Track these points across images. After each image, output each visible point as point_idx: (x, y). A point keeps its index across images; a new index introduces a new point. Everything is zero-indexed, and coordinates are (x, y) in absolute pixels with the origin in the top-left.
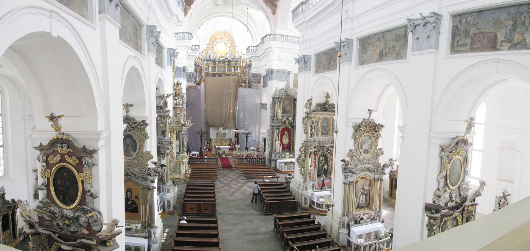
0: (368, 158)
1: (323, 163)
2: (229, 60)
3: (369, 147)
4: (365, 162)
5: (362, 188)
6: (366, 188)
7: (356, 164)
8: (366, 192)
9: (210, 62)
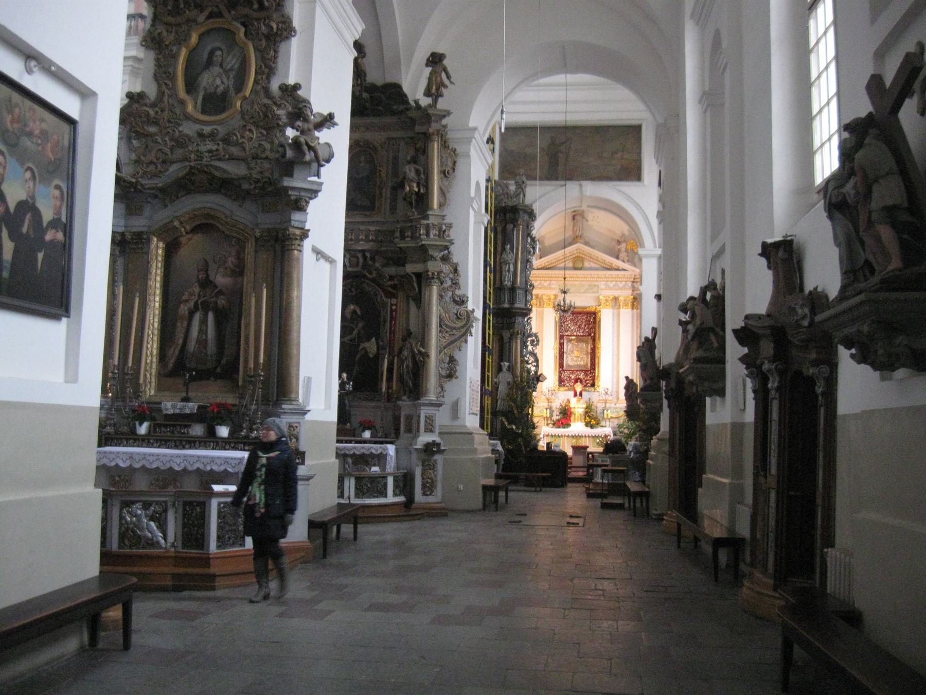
0: (222, 131)
1: (355, 332)
3: (231, 83)
4: (203, 148)
5: (202, 276)
6: (222, 280)
7: (160, 155)
8: (222, 301)
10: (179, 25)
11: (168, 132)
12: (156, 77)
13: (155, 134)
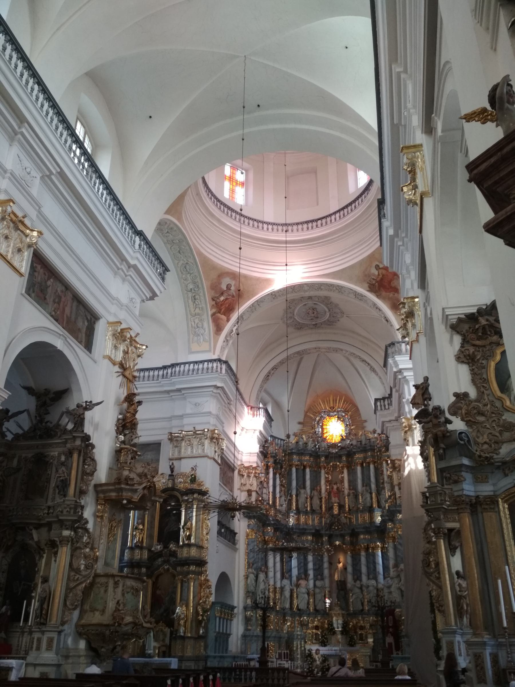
2: (349, 452)
9: (307, 458)
10: (484, 346)
11: (494, 421)
12: (473, 381)
13: (483, 422)
